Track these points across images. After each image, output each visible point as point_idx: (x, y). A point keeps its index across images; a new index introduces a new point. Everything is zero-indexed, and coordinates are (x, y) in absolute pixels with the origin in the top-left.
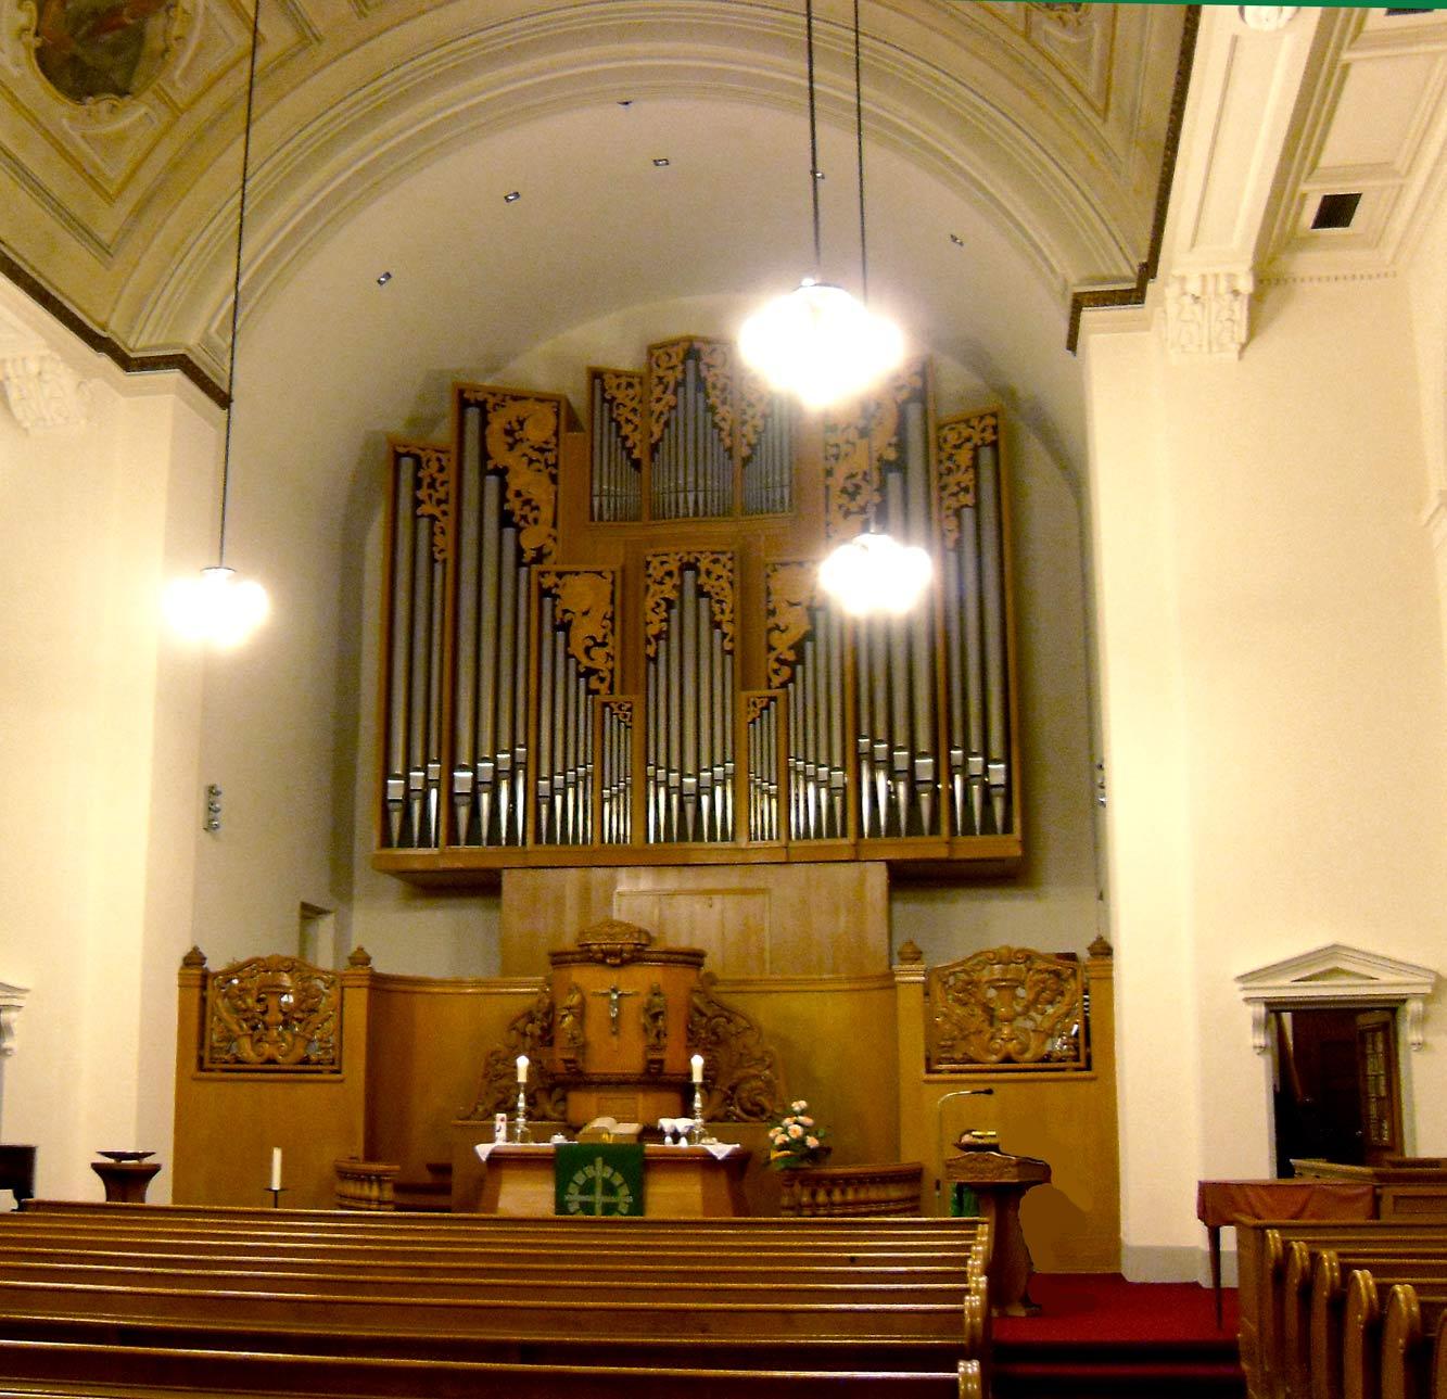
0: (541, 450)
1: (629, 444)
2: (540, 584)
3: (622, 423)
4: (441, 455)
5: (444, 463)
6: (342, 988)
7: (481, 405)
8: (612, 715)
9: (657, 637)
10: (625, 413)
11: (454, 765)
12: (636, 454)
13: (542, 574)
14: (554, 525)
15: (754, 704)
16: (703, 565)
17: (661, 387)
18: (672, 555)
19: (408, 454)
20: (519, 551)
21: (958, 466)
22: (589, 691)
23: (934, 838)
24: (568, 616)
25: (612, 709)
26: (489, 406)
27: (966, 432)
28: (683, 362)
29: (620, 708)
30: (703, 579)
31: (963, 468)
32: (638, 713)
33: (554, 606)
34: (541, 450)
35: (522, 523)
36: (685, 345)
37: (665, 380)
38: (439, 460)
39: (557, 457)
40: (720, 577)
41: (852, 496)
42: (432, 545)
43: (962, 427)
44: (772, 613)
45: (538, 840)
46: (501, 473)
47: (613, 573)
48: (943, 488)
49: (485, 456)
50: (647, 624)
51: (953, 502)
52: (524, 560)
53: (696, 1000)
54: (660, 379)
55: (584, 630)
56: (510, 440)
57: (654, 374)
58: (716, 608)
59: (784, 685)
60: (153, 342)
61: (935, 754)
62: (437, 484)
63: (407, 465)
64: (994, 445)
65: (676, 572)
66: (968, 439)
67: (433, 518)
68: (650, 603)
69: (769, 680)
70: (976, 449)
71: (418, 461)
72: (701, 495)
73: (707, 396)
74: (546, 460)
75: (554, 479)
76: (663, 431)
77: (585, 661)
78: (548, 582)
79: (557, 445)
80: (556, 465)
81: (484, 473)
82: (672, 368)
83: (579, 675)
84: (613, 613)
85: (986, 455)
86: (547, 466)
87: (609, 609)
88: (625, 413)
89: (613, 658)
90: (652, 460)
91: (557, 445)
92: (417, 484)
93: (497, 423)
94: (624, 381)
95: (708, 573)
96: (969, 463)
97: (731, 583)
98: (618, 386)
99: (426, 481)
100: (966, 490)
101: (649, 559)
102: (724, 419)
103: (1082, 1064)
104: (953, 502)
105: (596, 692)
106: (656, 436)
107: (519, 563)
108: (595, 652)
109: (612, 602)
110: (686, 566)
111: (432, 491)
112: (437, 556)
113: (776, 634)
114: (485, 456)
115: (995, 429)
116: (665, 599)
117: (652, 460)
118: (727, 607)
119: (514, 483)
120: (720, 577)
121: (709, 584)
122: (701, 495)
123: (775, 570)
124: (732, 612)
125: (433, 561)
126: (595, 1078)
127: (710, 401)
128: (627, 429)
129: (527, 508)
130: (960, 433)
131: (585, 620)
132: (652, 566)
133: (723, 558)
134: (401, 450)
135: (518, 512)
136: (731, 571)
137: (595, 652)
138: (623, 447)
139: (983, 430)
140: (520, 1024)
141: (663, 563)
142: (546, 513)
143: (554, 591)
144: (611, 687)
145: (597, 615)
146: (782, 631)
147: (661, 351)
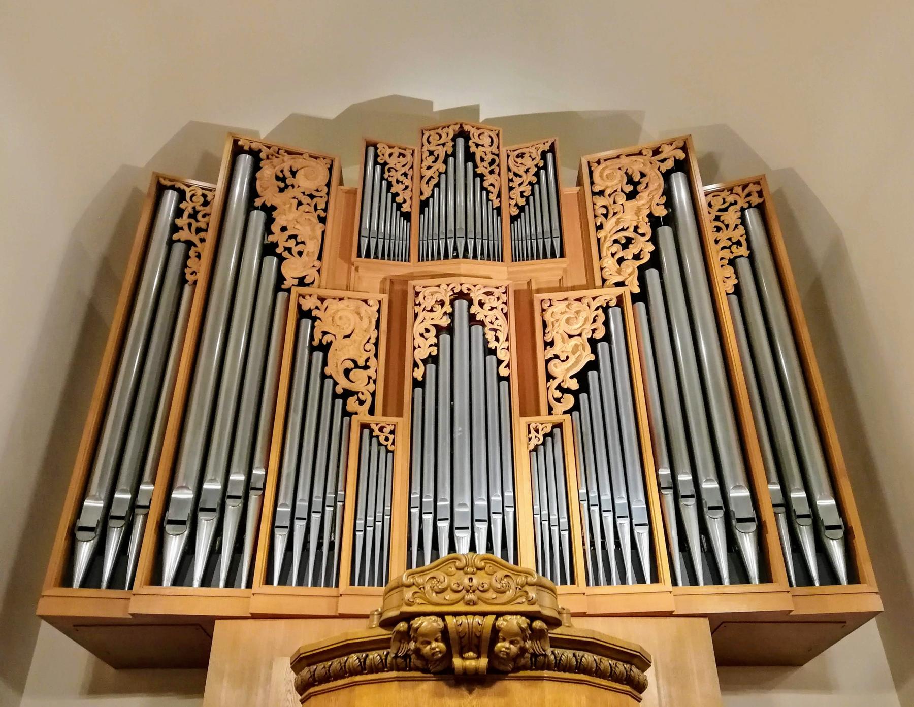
0: (312, 197)
2: (299, 306)
3: (394, 183)
4: (206, 192)
5: (209, 199)
7: (255, 155)
8: (371, 437)
9: (425, 362)
12: (406, 208)
14: (320, 258)
15: (537, 431)
16: (476, 296)
17: (432, 158)
18: (444, 286)
19: (172, 188)
20: (280, 278)
21: (727, 226)
22: (346, 413)
25: (372, 431)
28: (454, 139)
29: (381, 430)
30: (475, 309)
31: (732, 227)
33: (313, 327)
34: (312, 197)
35: (286, 254)
36: (457, 128)
37: (436, 153)
38: (204, 196)
39: (327, 203)
40: (492, 308)
41: (625, 246)
42: (184, 265)
43: (726, 193)
44: (551, 344)
45: (268, 580)
46: (269, 210)
47: (380, 302)
48: (717, 242)
49: (253, 193)
50: (415, 348)
51: (726, 254)
52: (283, 287)
54: (431, 153)
56: (282, 185)
57: (425, 149)
58: (490, 336)
62: (199, 216)
65: (447, 302)
66: (736, 203)
67: (189, 244)
68: (419, 328)
69: (550, 409)
70: (743, 210)
73: (475, 166)
74: (315, 206)
75: (323, 220)
76: (433, 191)
78: (307, 304)
79: (328, 194)
80: (325, 210)
81: (250, 207)
82: (444, 144)
83: (335, 396)
84: (377, 339)
85: (752, 216)
87: (374, 335)
88: (394, 176)
89: (375, 382)
91: (328, 194)
92: (179, 213)
93: (267, 172)
94: (396, 151)
95: (481, 304)
96: (739, 221)
97: (506, 314)
98: (390, 155)
99: (189, 210)
100: (739, 243)
101: (418, 289)
104: (726, 254)
106: (427, 194)
107: (278, 288)
108: (355, 374)
109: (377, 327)
110: (461, 295)
111: (192, 221)
112: (188, 277)
113: (557, 361)
115: (760, 194)
116: (436, 326)
117: (422, 212)
118: (502, 337)
119: (280, 220)
123: (551, 305)
124: (507, 340)
125: (183, 281)
127: (479, 171)
130: (724, 199)
132: (421, 296)
133: (497, 293)
134: (168, 183)
136: (506, 303)
137: (355, 374)
138: (393, 201)
139: (749, 195)
142: (312, 247)
143: (314, 314)
144: (371, 411)
146: (563, 361)
147: (432, 133)
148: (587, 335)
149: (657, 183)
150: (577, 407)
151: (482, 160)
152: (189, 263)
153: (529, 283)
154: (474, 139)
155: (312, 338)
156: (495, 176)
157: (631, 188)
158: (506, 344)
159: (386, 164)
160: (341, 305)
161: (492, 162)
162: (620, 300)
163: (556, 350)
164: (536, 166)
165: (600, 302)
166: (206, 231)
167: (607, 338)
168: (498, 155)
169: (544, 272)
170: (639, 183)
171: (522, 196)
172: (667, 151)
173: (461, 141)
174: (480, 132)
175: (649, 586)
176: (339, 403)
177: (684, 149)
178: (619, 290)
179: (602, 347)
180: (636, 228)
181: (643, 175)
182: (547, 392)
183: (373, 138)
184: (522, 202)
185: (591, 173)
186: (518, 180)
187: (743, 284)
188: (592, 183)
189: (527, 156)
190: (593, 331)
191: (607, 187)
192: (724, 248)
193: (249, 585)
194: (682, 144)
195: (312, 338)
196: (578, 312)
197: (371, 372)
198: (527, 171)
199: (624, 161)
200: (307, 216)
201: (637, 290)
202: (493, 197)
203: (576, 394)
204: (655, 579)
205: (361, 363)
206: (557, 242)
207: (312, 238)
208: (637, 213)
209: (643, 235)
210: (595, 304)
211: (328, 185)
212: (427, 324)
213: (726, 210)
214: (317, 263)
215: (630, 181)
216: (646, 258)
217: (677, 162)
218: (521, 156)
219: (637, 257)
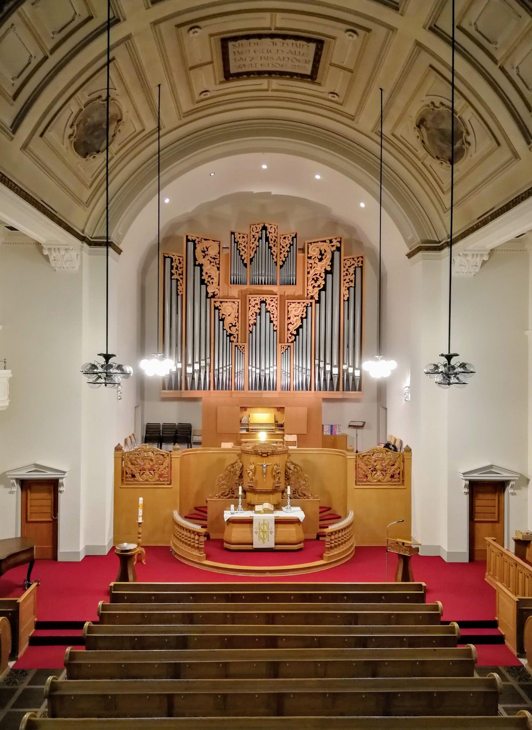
0: (214, 259)
1: (243, 258)
3: (241, 251)
5: (181, 261)
6: (171, 458)
7: (194, 241)
10: (242, 247)
11: (186, 365)
12: (245, 262)
13: (215, 302)
14: (219, 285)
17: (254, 239)
18: (258, 298)
19: (169, 257)
20: (207, 293)
22: (230, 341)
23: (338, 392)
24: (224, 316)
26: (196, 242)
27: (353, 262)
28: (261, 231)
30: (267, 306)
32: (246, 349)
33: (219, 313)
34: (214, 259)
35: (208, 284)
38: (179, 259)
40: (273, 306)
41: (316, 282)
42: (177, 289)
43: (352, 260)
44: (289, 318)
45: (214, 389)
46: (201, 266)
48: (345, 280)
49: (195, 259)
53: (288, 464)
55: (229, 320)
56: (204, 255)
58: (272, 316)
59: (292, 342)
60: (99, 235)
61: (339, 367)
62: (179, 268)
63: (168, 261)
64: (361, 267)
66: (353, 265)
67: (177, 280)
68: (250, 313)
69: (288, 340)
70: (355, 268)
71: (172, 259)
72: (267, 278)
73: (269, 243)
75: (218, 269)
77: (229, 330)
78: (217, 304)
80: (219, 264)
81: (195, 265)
82: (258, 232)
83: (227, 336)
85: (358, 270)
86: (216, 264)
88: (242, 247)
90: (251, 264)
92: (172, 268)
94: (241, 235)
98: (240, 237)
100: (352, 281)
102: (274, 252)
103: (401, 483)
105: (233, 341)
106: (252, 256)
107: (207, 297)
109: (238, 312)
110: (262, 302)
112: (179, 293)
113: (290, 325)
114: (195, 259)
116: (255, 312)
117: (251, 264)
118: (275, 317)
119: (205, 269)
120: (273, 306)
121: (269, 308)
122: (267, 278)
125: (178, 295)
126: (258, 491)
127: (270, 245)
128: (242, 253)
129: (210, 278)
131: (229, 317)
134: (166, 255)
135: (206, 280)
138: (241, 259)
139: (359, 262)
140: (228, 468)
141: (255, 300)
142: (216, 280)
145: (233, 315)
147: (254, 226)
148: (300, 316)
149: (329, 256)
150: (295, 340)
151: (271, 240)
152: (179, 288)
153: (285, 293)
154: (269, 230)
155: (219, 317)
156: (276, 247)
157: (320, 257)
158: (276, 319)
159: (238, 242)
160: (227, 304)
161: (274, 242)
162: (311, 303)
163: (291, 321)
164: (290, 243)
165: (305, 304)
166: (182, 274)
167: (306, 317)
168: (277, 237)
169: (289, 290)
170: (323, 255)
171: (284, 257)
172: (335, 242)
173: (264, 231)
174: (271, 226)
175: (308, 391)
176: (228, 338)
177: (340, 242)
178: (311, 301)
179: (305, 320)
180: (320, 274)
181: (325, 251)
182: (287, 335)
183: (233, 230)
184: (284, 259)
185: (308, 248)
186: (283, 249)
187: (350, 298)
188: (308, 253)
189: (287, 238)
190: (302, 315)
191: (313, 255)
192: (347, 282)
193: (209, 389)
194: (339, 240)
195: (219, 317)
196: (298, 308)
197: (237, 327)
198: (286, 246)
199: (320, 244)
200: (213, 267)
201: (317, 299)
202: (274, 257)
203: (295, 336)
204: (310, 390)
205: (234, 324)
206: (294, 278)
207: (216, 276)
208: (321, 268)
209: (322, 277)
210: (303, 305)
211: (219, 253)
212: (253, 312)
213: (350, 267)
214: (218, 287)
215: (321, 254)
216: (322, 287)
217: (337, 247)
218: (285, 238)
219: (319, 286)
